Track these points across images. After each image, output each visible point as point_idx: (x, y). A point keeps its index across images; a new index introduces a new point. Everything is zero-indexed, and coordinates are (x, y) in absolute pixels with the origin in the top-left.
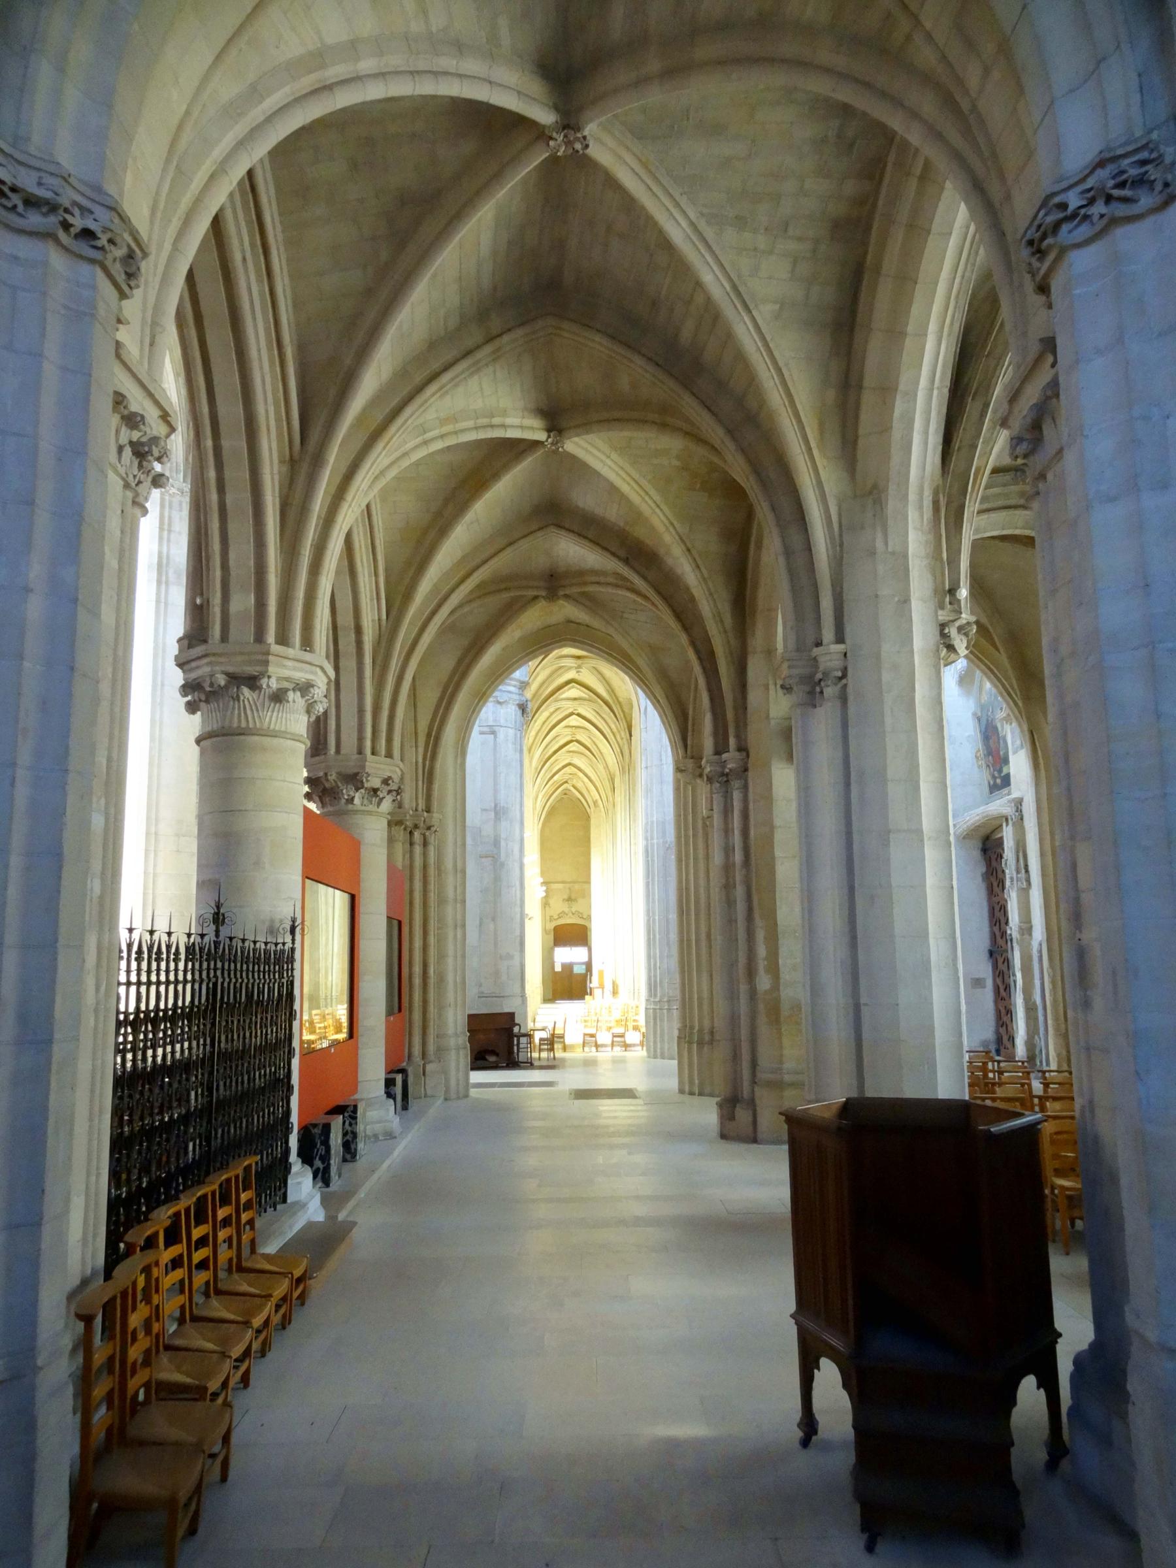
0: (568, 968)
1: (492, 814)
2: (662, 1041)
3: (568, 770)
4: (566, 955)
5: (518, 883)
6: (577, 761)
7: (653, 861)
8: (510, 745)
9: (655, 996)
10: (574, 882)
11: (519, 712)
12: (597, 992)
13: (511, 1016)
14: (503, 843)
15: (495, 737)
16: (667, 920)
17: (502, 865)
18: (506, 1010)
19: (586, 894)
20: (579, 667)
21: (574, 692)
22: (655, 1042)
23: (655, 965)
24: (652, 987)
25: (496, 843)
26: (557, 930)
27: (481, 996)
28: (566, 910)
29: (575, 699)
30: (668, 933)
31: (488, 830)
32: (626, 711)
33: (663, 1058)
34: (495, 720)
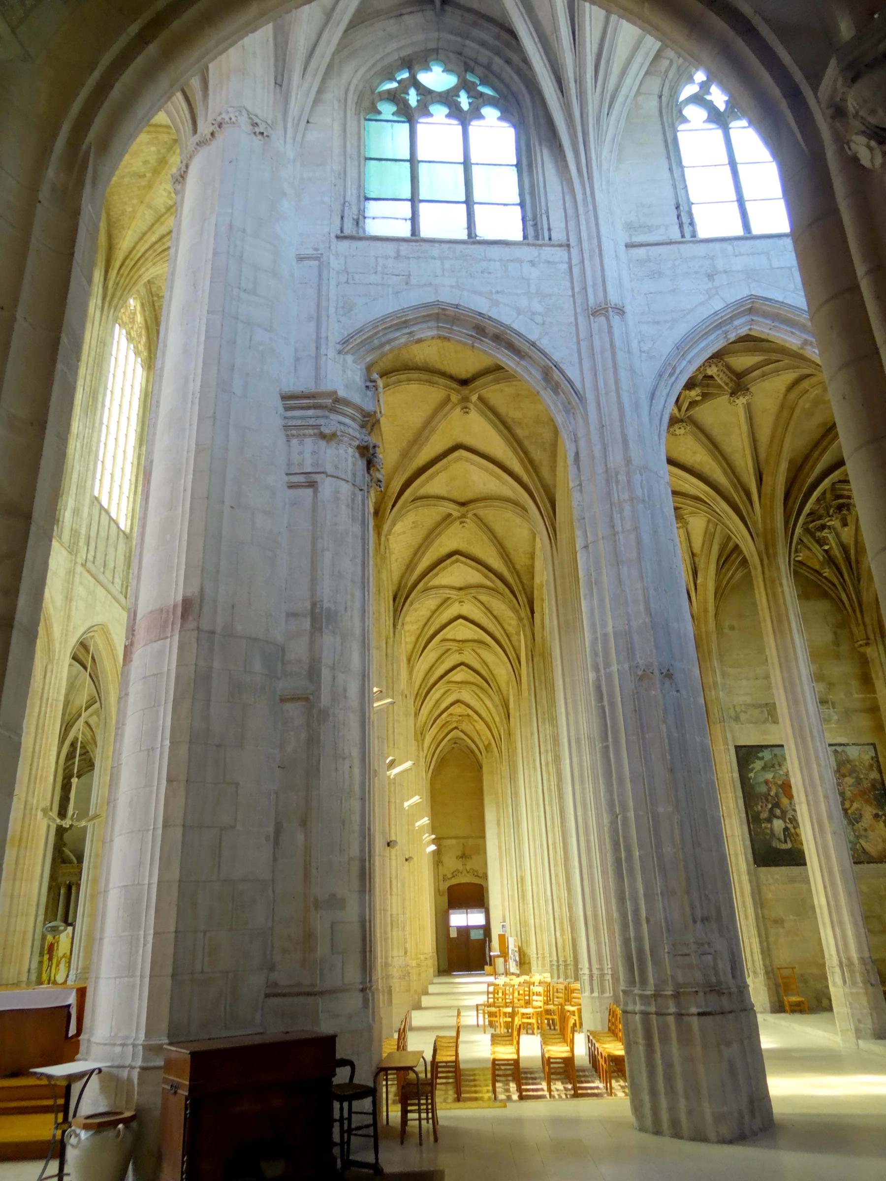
0: (464, 931)
1: (307, 623)
2: (671, 1089)
3: (458, 710)
4: (458, 919)
5: (355, 753)
6: (466, 695)
7: (612, 704)
8: (343, 508)
9: (644, 982)
10: (466, 838)
11: (361, 464)
12: (500, 962)
13: (329, 1042)
14: (326, 674)
15: (316, 492)
16: (656, 818)
17: (324, 715)
18: (326, 1028)
19: (481, 850)
20: (464, 516)
21: (458, 574)
22: (653, 1093)
23: (636, 912)
24: (634, 962)
25: (313, 673)
26: (450, 889)
27: (273, 992)
28: (461, 868)
29: (461, 589)
30: (659, 845)
31: (298, 650)
32: (525, 581)
33: (677, 1134)
34: (315, 464)
